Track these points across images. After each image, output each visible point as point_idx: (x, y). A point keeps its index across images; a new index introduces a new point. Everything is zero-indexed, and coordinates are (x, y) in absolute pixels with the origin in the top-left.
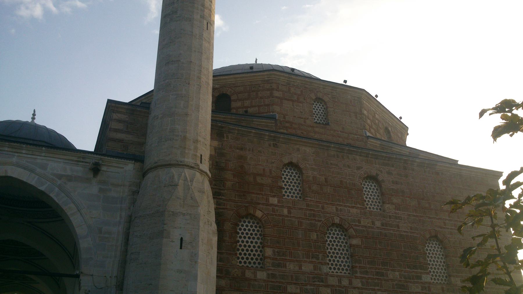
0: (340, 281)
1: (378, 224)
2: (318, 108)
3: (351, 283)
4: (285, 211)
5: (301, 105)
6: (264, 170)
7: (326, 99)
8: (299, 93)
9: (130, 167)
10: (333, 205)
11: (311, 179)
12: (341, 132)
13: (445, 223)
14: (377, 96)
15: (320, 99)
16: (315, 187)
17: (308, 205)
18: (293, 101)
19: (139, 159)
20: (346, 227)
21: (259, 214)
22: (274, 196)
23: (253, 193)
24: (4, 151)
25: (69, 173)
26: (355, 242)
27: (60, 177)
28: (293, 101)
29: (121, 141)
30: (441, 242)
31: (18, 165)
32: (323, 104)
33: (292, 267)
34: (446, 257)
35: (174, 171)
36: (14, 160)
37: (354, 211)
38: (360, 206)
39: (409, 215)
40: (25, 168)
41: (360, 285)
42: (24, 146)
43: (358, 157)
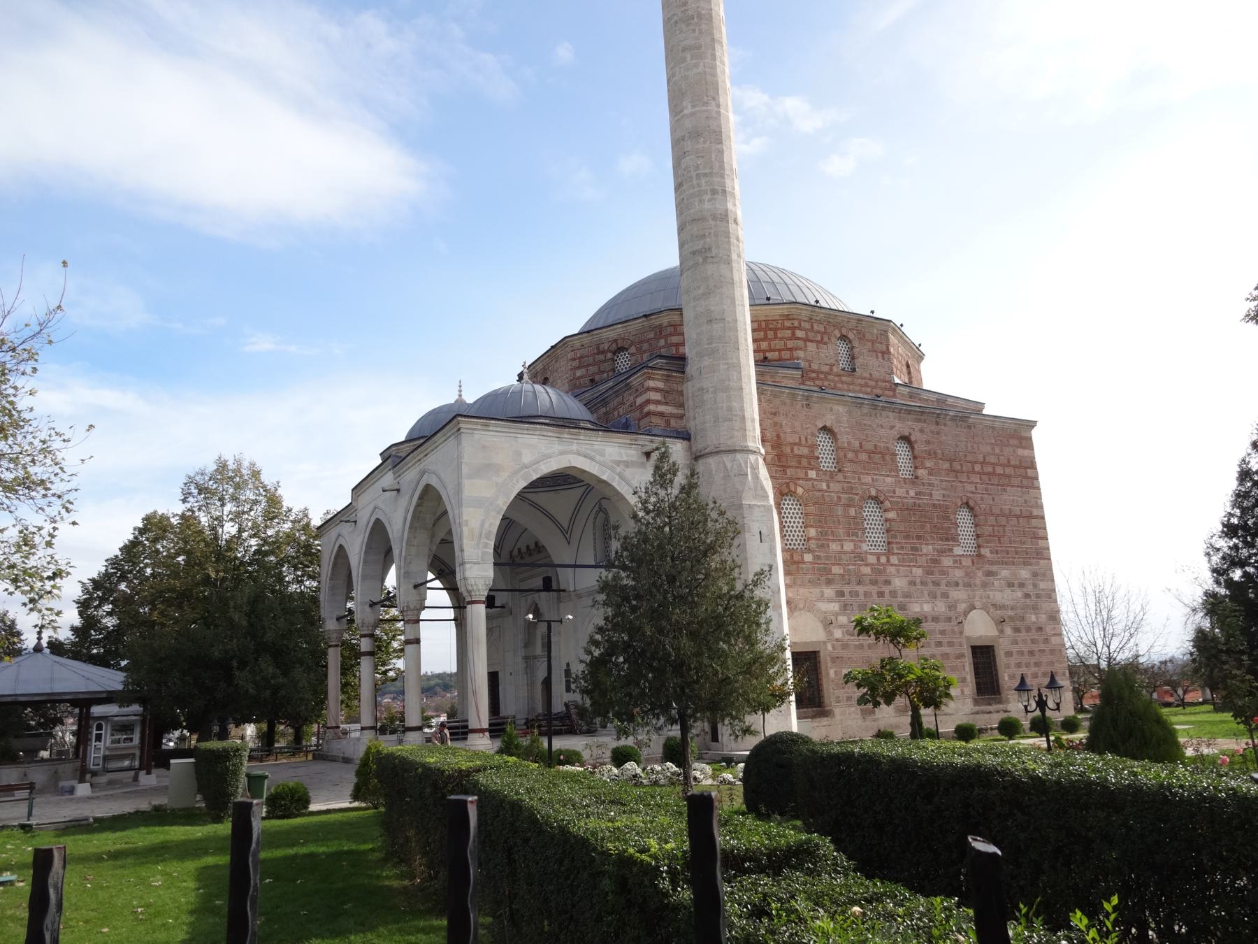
0: (878, 559)
2: (842, 348)
3: (888, 560)
4: (824, 486)
7: (851, 336)
17: (845, 477)
18: (817, 342)
19: (686, 436)
21: (800, 491)
25: (625, 458)
26: (892, 515)
27: (618, 463)
28: (817, 342)
29: (661, 415)
30: (971, 509)
33: (834, 547)
34: (976, 526)
35: (738, 456)
36: (575, 447)
37: (889, 480)
41: (896, 562)
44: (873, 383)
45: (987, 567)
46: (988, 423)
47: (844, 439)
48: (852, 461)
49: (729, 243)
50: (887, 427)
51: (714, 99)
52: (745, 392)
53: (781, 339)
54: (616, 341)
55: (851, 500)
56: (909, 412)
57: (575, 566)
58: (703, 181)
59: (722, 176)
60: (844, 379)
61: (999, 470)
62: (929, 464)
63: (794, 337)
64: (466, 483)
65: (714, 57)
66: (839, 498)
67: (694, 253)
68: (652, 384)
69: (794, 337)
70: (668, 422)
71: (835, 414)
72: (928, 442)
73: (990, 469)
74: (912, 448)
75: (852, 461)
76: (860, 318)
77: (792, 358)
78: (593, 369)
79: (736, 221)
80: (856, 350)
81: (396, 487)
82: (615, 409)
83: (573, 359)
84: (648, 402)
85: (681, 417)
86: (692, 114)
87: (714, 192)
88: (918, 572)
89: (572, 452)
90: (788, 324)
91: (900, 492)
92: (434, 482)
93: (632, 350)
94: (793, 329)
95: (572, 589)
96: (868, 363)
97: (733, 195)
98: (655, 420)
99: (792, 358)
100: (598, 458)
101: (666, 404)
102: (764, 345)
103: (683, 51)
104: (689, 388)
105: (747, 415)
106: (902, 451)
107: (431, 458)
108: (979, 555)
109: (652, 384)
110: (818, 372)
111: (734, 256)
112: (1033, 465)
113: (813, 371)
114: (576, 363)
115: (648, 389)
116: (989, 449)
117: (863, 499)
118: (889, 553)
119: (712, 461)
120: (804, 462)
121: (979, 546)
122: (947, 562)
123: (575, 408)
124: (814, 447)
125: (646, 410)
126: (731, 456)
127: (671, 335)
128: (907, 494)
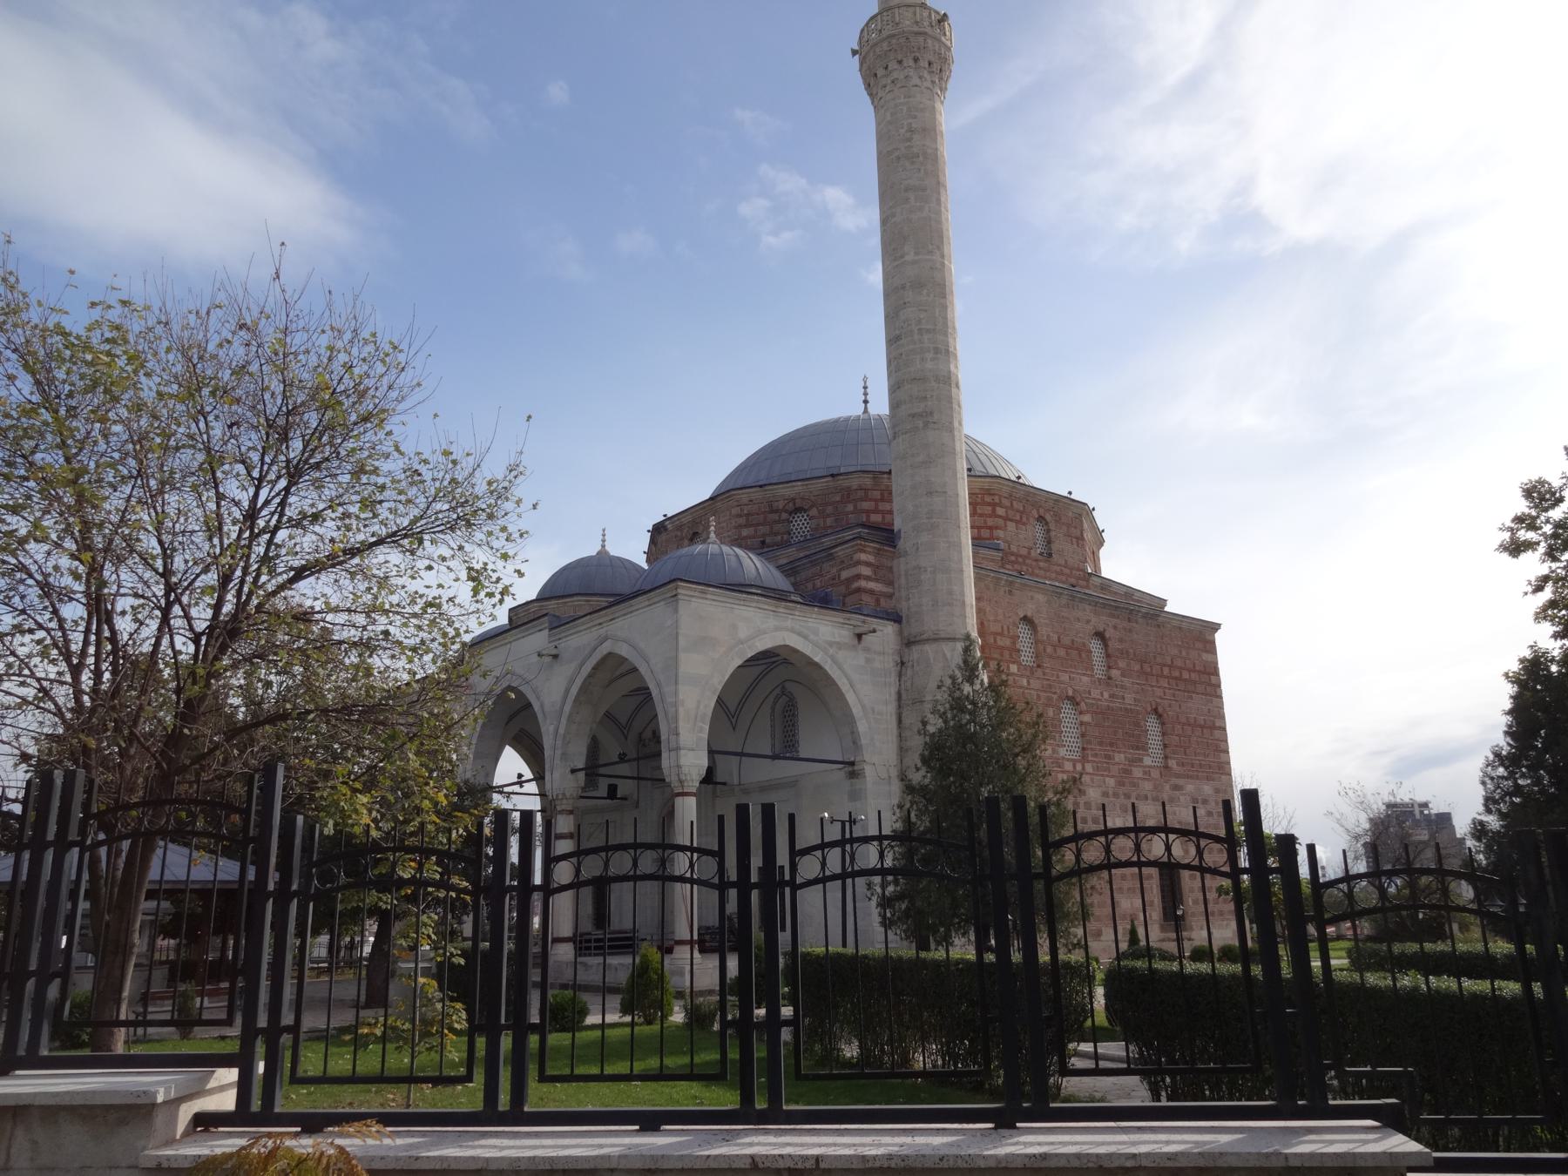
2: (1039, 531)
4: (1025, 682)
7: (1048, 517)
9: (888, 630)
16: (1049, 650)
18: (1017, 522)
19: (896, 618)
26: (1087, 718)
27: (831, 644)
29: (871, 592)
30: (1160, 716)
31: (792, 630)
34: (1164, 734)
36: (789, 623)
37: (1085, 679)
40: (799, 634)
44: (1067, 571)
45: (1174, 781)
46: (1175, 623)
47: (1043, 631)
50: (1085, 620)
53: (981, 515)
54: (793, 500)
55: (1050, 699)
56: (1104, 606)
57: (741, 754)
58: (926, 337)
59: (946, 334)
61: (1186, 675)
62: (1122, 664)
63: (994, 515)
64: (682, 656)
65: (939, 201)
66: (1039, 697)
67: (913, 416)
68: (863, 557)
69: (994, 515)
70: (878, 601)
71: (1035, 603)
72: (1121, 640)
73: (1176, 674)
74: (1106, 646)
75: (1050, 657)
77: (991, 538)
78: (763, 529)
81: (554, 652)
82: (807, 580)
83: (739, 516)
84: (858, 577)
85: (891, 596)
86: (914, 262)
87: (937, 351)
88: (1111, 782)
89: (787, 629)
90: (988, 499)
91: (1095, 693)
92: (623, 650)
93: (814, 512)
94: (993, 505)
95: (736, 782)
96: (1061, 544)
98: (866, 598)
99: (991, 538)
101: (877, 580)
103: (906, 190)
104: (901, 566)
106: (1095, 647)
107: (619, 623)
108: (1166, 767)
109: (863, 557)
110: (1017, 555)
111: (956, 424)
112: (1214, 671)
114: (742, 521)
115: (859, 563)
116: (1175, 651)
117: (1061, 699)
118: (1084, 759)
119: (929, 649)
120: (1006, 653)
121: (1166, 757)
122: (1137, 772)
124: (1015, 638)
125: (855, 585)
126: (951, 644)
127: (862, 500)
128: (1100, 695)
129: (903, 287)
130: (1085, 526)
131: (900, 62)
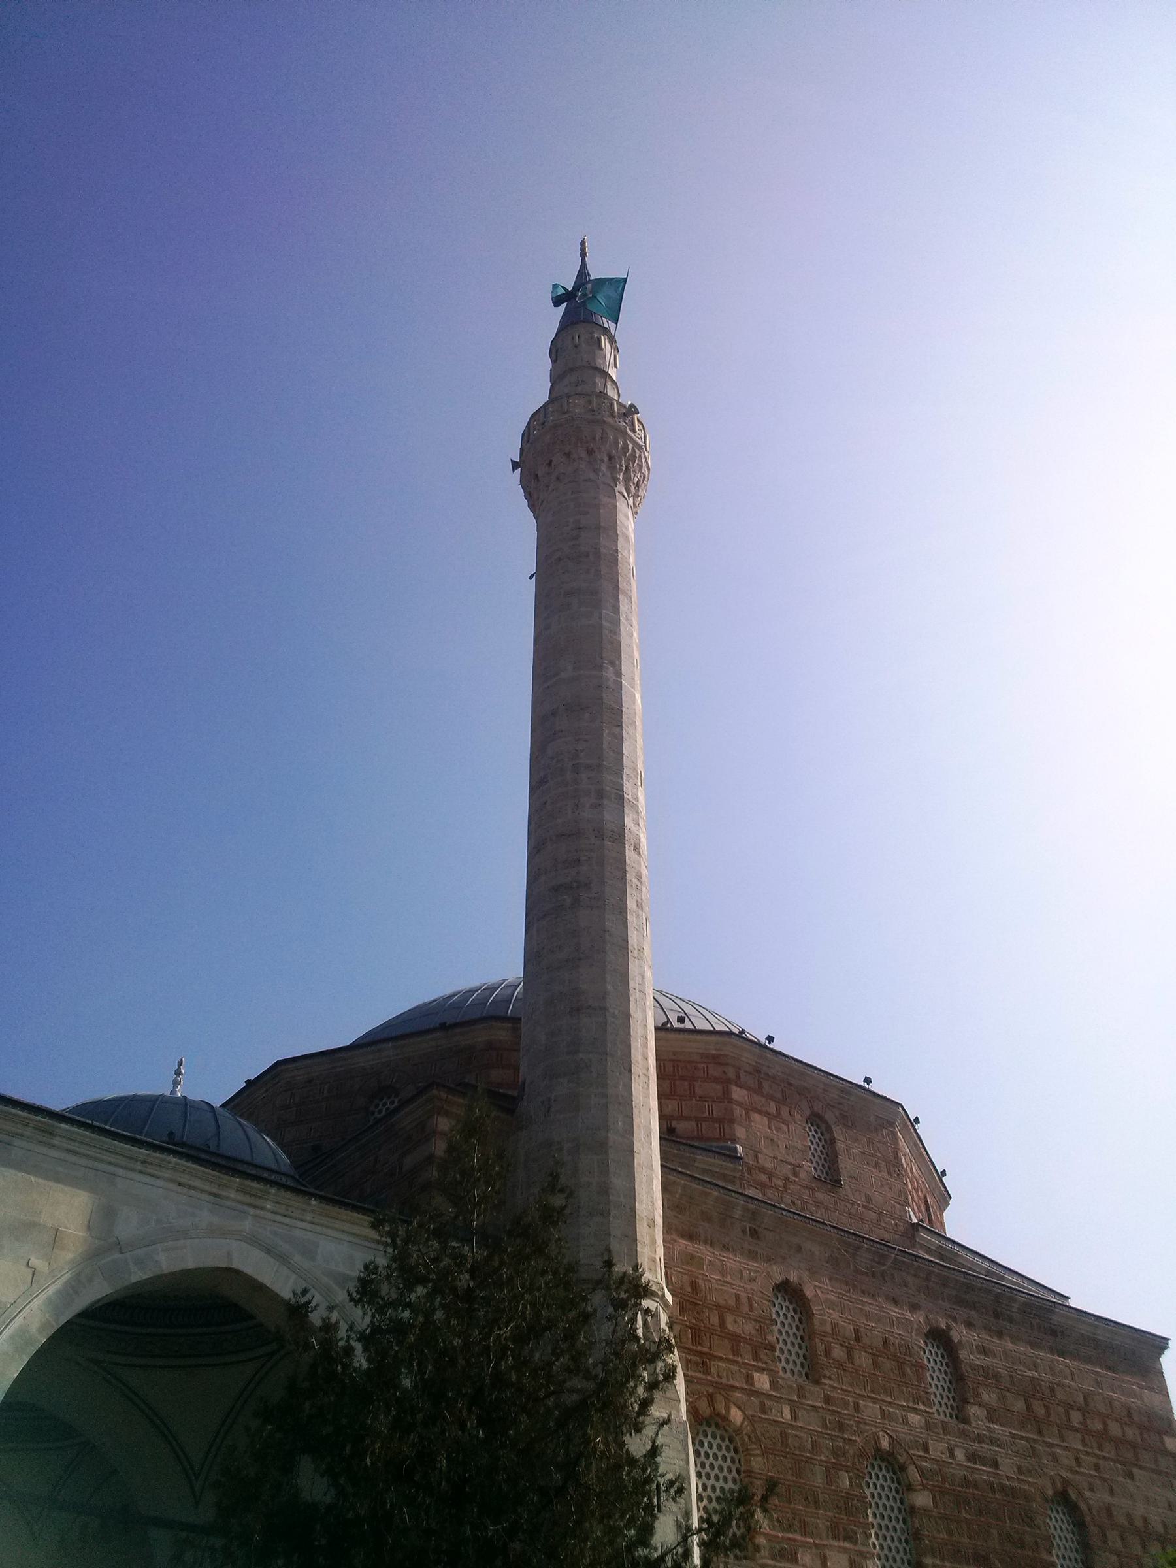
1: (960, 1455)
5: (784, 1127)
6: (737, 1297)
7: (829, 1116)
8: (779, 1096)
10: (874, 1401)
11: (828, 1329)
12: (864, 1207)
13: (1077, 1459)
14: (917, 1120)
15: (818, 1116)
16: (838, 1352)
17: (828, 1399)
18: (767, 1114)
20: (902, 1460)
21: (736, 1415)
22: (761, 1370)
23: (721, 1359)
24: (227, 1198)
32: (823, 1127)
36: (247, 1225)
37: (915, 1419)
38: (923, 1408)
39: (1013, 1436)
40: (268, 1251)
42: (273, 1191)
43: (910, 1280)
48: (840, 1365)
49: (623, 879)
51: (612, 663)
52: (639, 1159)
53: (703, 1099)
60: (820, 1196)
62: (988, 1396)
67: (556, 889)
69: (726, 1096)
73: (1097, 1426)
76: (845, 1088)
79: (637, 849)
80: (840, 1145)
90: (715, 1071)
97: (636, 809)
100: (297, 1258)
102: (672, 1106)
105: (641, 1208)
110: (771, 1175)
111: (631, 904)
113: (762, 1170)
120: (746, 1349)
123: (268, 1149)
128: (949, 1453)
129: (554, 713)
130: (902, 1142)
131: (568, 455)
